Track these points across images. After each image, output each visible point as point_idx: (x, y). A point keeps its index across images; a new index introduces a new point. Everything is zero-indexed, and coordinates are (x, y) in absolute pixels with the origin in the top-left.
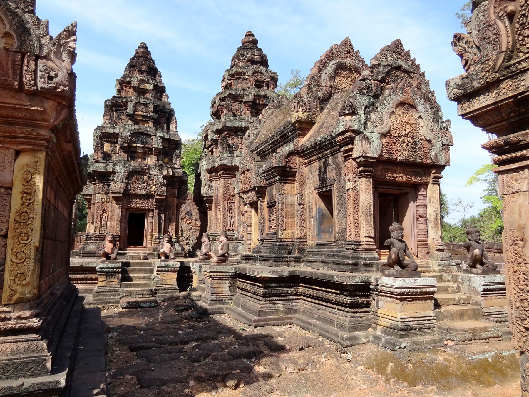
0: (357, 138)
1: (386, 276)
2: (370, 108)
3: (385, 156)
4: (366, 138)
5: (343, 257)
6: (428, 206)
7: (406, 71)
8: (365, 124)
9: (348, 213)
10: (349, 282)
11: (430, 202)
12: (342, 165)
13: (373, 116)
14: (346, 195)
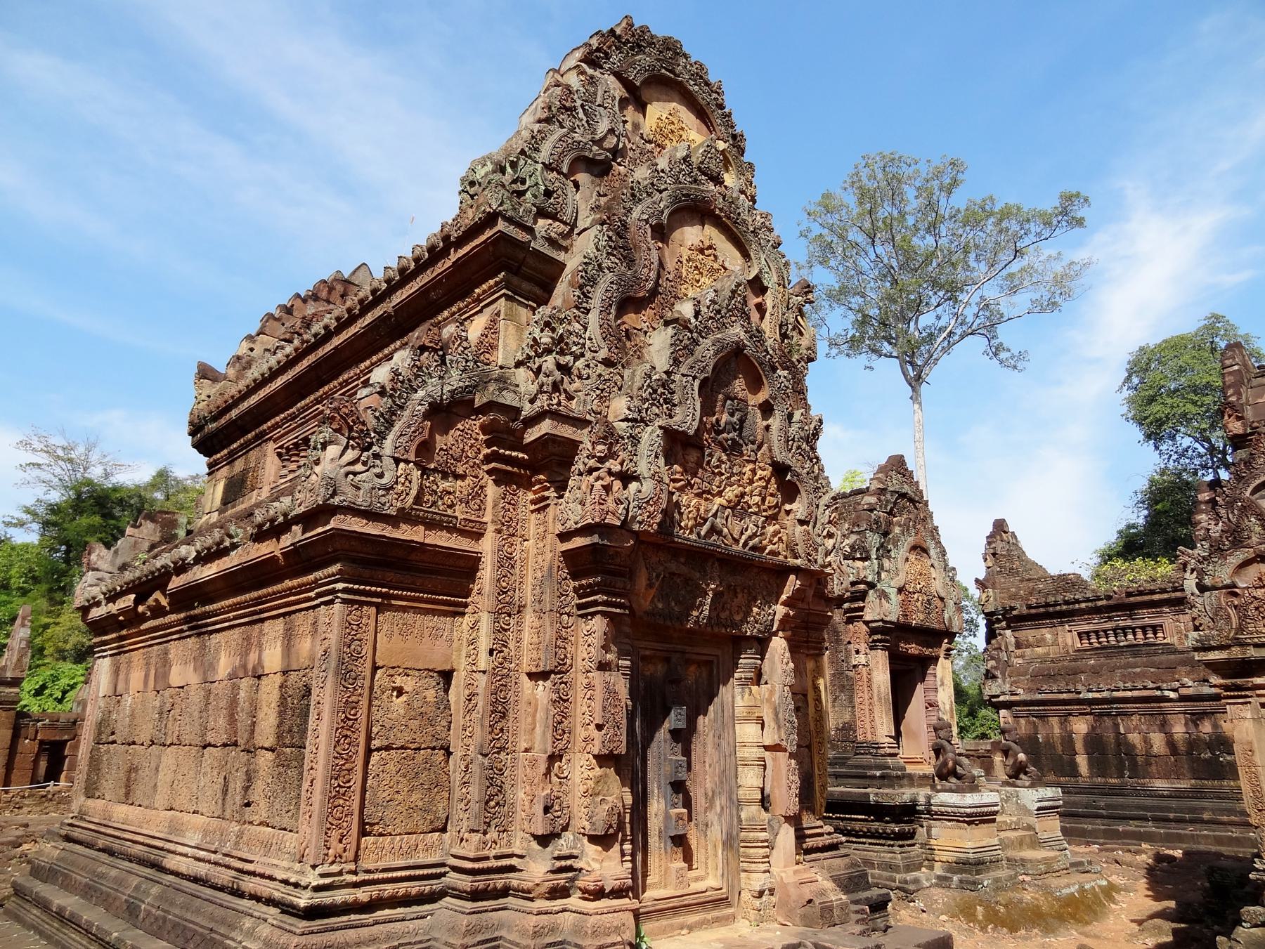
0: (871, 592)
1: (938, 791)
2: (884, 551)
3: (902, 620)
4: (884, 595)
5: (856, 767)
6: (940, 689)
7: (911, 500)
8: (879, 574)
9: (857, 700)
10: (898, 801)
11: (942, 684)
12: (841, 627)
13: (886, 563)
14: (851, 674)
